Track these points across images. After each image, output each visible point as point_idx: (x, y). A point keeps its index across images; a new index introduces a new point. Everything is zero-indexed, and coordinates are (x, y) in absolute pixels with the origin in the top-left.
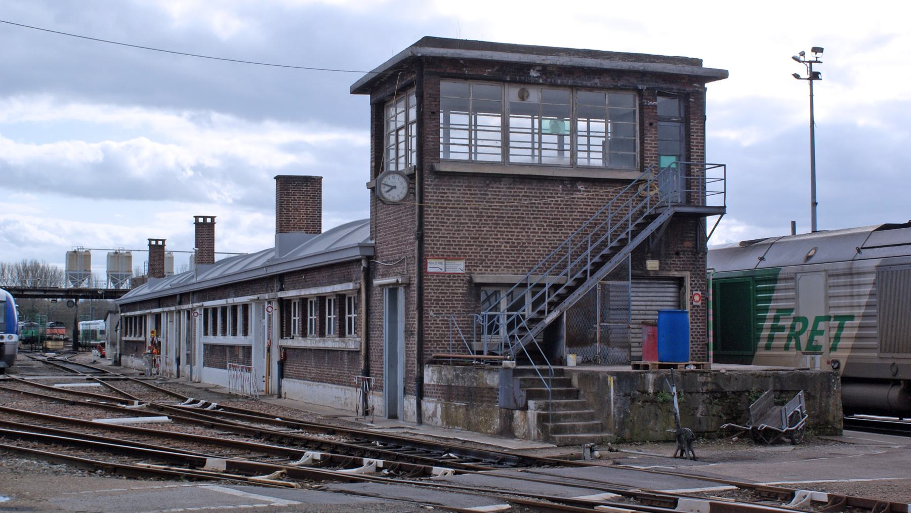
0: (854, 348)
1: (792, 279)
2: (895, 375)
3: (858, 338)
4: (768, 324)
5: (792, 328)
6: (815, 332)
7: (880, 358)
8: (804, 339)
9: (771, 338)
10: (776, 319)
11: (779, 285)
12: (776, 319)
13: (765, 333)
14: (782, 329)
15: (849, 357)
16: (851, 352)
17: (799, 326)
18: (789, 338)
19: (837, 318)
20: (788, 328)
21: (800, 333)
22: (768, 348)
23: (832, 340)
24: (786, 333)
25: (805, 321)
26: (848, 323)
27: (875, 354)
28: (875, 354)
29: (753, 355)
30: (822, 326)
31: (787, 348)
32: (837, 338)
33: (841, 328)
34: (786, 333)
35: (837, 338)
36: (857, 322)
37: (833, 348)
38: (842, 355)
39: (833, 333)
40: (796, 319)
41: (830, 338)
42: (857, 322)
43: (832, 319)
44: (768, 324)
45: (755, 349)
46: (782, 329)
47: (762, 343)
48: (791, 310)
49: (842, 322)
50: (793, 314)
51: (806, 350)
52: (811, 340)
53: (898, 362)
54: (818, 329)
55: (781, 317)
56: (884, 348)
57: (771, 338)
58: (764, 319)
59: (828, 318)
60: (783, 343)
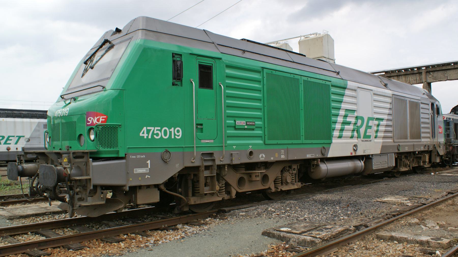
0: (384, 137)
1: (355, 90)
3: (386, 131)
4: (340, 119)
5: (355, 124)
6: (368, 127)
8: (362, 130)
9: (342, 130)
10: (346, 116)
11: (347, 92)
12: (346, 116)
14: (349, 123)
15: (383, 142)
17: (359, 122)
18: (353, 131)
19: (377, 119)
20: (352, 124)
22: (340, 137)
24: (351, 127)
25: (362, 119)
26: (382, 123)
30: (371, 123)
31: (352, 137)
32: (377, 131)
33: (378, 125)
34: (351, 127)
35: (377, 131)
36: (384, 123)
39: (375, 128)
40: (357, 118)
42: (384, 123)
44: (340, 119)
46: (349, 123)
47: (336, 133)
48: (354, 111)
49: (379, 122)
50: (356, 114)
52: (366, 132)
53: (400, 144)
55: (349, 115)
57: (342, 130)
59: (372, 119)
60: (350, 134)
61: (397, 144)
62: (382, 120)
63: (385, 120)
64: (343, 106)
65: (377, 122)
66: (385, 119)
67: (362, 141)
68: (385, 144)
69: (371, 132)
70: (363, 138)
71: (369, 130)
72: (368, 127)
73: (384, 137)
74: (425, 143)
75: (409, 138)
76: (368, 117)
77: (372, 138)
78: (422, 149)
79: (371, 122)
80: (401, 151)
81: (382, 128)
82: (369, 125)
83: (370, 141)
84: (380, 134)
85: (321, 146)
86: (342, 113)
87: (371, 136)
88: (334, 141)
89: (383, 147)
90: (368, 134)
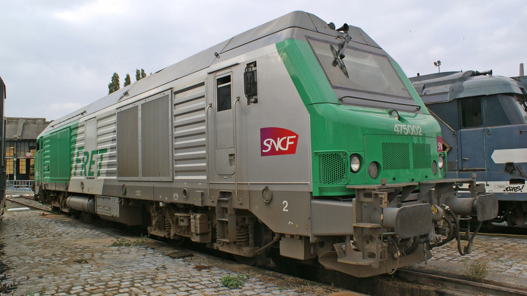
0: (108, 173)
2: (125, 194)
3: (109, 165)
7: (118, 181)
8: (88, 166)
13: (74, 165)
16: (106, 176)
21: (86, 163)
22: (75, 174)
23: (99, 167)
26: (105, 154)
27: (115, 178)
28: (115, 178)
29: (70, 180)
31: (81, 174)
33: (102, 158)
36: (108, 153)
37: (99, 174)
38: (103, 177)
41: (98, 166)
42: (108, 153)
43: (99, 152)
44: (75, 158)
45: (70, 175)
47: (73, 171)
51: (88, 176)
53: (127, 184)
54: (93, 160)
55: (80, 153)
56: (120, 173)
58: (73, 155)
59: (95, 152)
61: (122, 184)
62: (105, 150)
63: (109, 149)
64: (78, 145)
65: (99, 155)
66: (107, 148)
67: (87, 178)
68: (108, 184)
69: (94, 169)
70: (88, 176)
71: (93, 166)
72: (92, 162)
73: (108, 173)
74: (185, 186)
75: (140, 174)
76: (92, 151)
77: (95, 174)
78: (176, 198)
79: (94, 155)
80: (128, 196)
81: (105, 161)
82: (93, 160)
83: (93, 178)
84: (104, 169)
85: (65, 182)
86: (76, 151)
87: (94, 172)
88: (73, 178)
89: (105, 187)
90: (92, 171)
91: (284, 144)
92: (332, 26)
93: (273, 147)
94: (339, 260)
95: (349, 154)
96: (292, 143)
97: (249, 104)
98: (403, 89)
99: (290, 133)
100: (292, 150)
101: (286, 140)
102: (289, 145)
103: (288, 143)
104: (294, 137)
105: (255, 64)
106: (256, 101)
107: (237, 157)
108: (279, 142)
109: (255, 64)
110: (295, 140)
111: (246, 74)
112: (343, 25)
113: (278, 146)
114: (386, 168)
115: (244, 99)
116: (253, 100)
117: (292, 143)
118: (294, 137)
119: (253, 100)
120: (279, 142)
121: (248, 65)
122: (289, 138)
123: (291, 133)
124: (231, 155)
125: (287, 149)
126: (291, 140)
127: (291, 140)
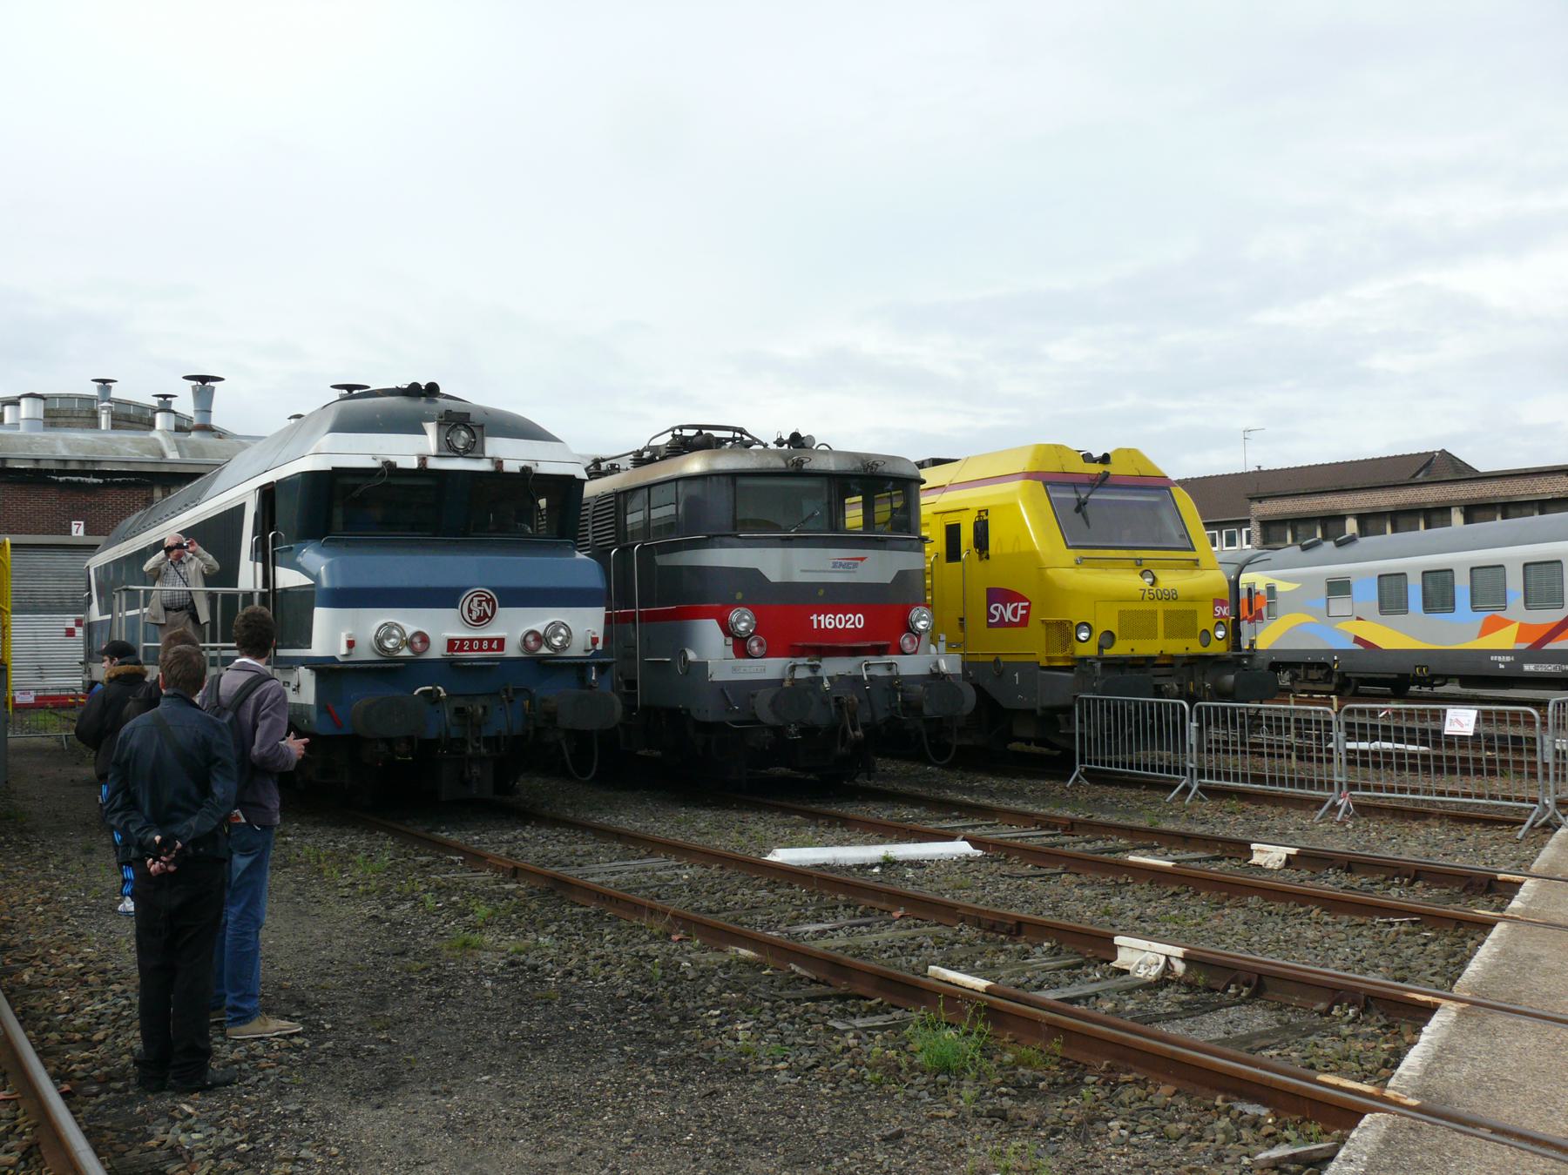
91: (1014, 613)
92: (1088, 458)
93: (1002, 616)
94: (1061, 731)
95: (1076, 623)
96: (1024, 612)
97: (981, 559)
98: (1182, 536)
99: (1022, 599)
100: (1025, 621)
101: (1017, 607)
102: (1021, 615)
103: (1020, 612)
104: (1027, 604)
105: (987, 512)
106: (988, 557)
107: (967, 622)
108: (1010, 608)
109: (987, 512)
110: (1027, 608)
111: (975, 523)
112: (1101, 455)
113: (1008, 615)
114: (1122, 637)
115: (974, 553)
116: (984, 556)
117: (1024, 612)
118: (1027, 604)
119: (984, 556)
120: (1010, 608)
121: (980, 511)
122: (1021, 604)
123: (1023, 599)
124: (962, 619)
125: (1018, 620)
126: (1023, 608)
127: (1023, 608)
